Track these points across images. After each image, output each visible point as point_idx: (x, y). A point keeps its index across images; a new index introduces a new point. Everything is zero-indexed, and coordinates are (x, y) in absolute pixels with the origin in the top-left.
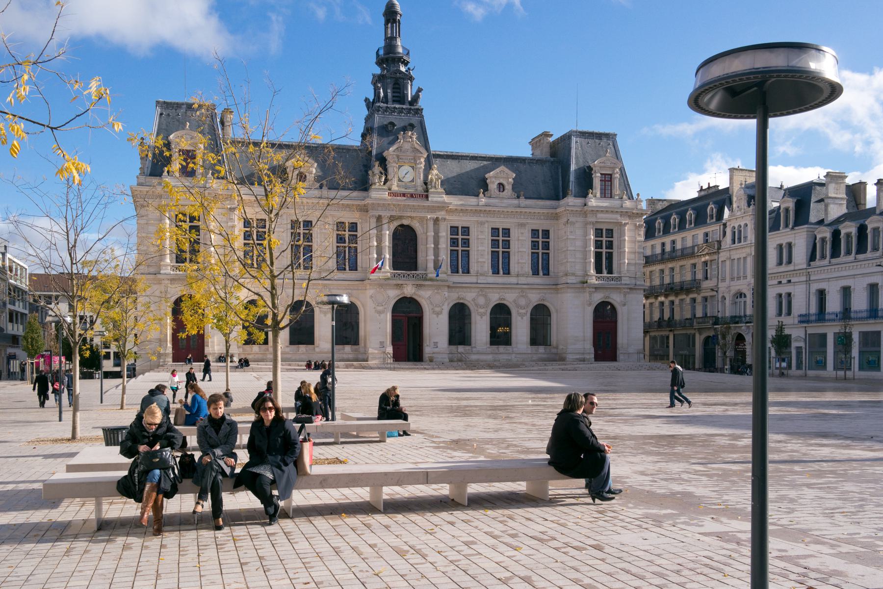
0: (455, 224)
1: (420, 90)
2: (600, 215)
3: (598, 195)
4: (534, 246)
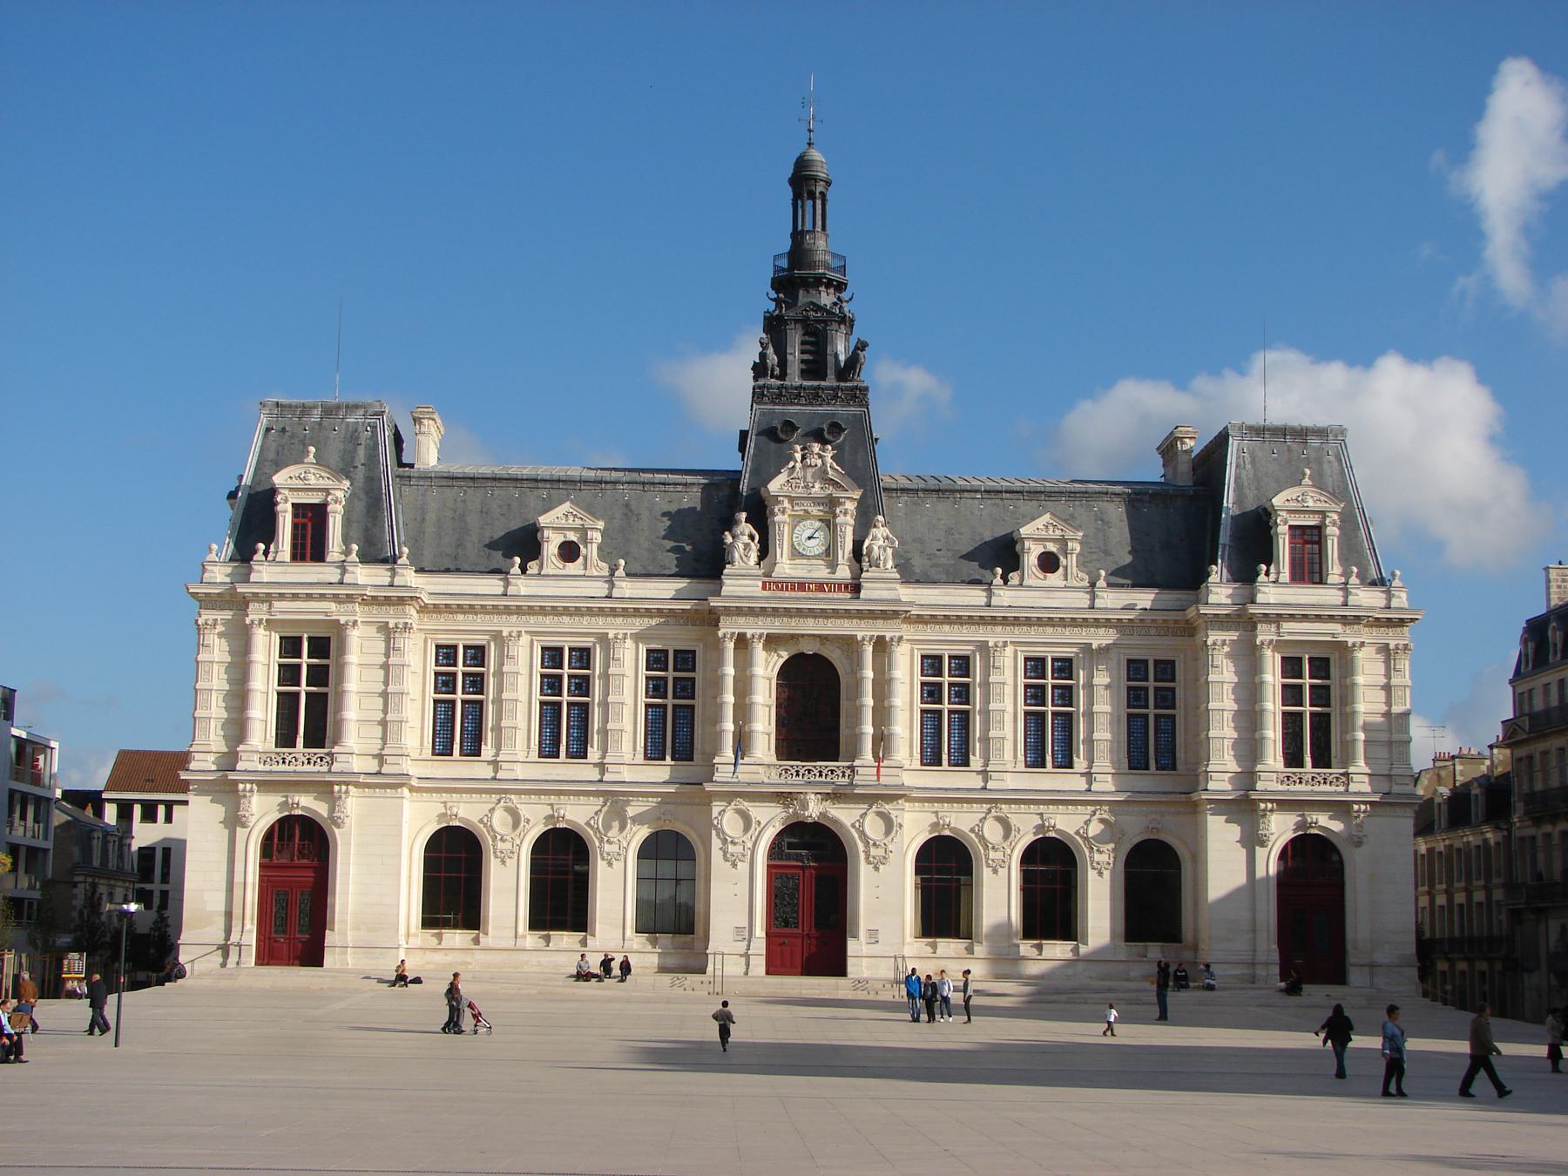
0: (1037, 651)
1: (862, 346)
2: (1287, 626)
3: (1285, 576)
4: (1137, 698)
